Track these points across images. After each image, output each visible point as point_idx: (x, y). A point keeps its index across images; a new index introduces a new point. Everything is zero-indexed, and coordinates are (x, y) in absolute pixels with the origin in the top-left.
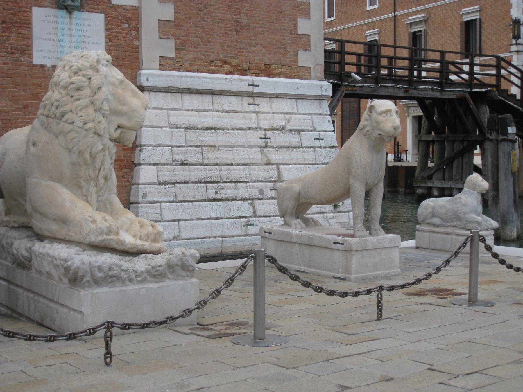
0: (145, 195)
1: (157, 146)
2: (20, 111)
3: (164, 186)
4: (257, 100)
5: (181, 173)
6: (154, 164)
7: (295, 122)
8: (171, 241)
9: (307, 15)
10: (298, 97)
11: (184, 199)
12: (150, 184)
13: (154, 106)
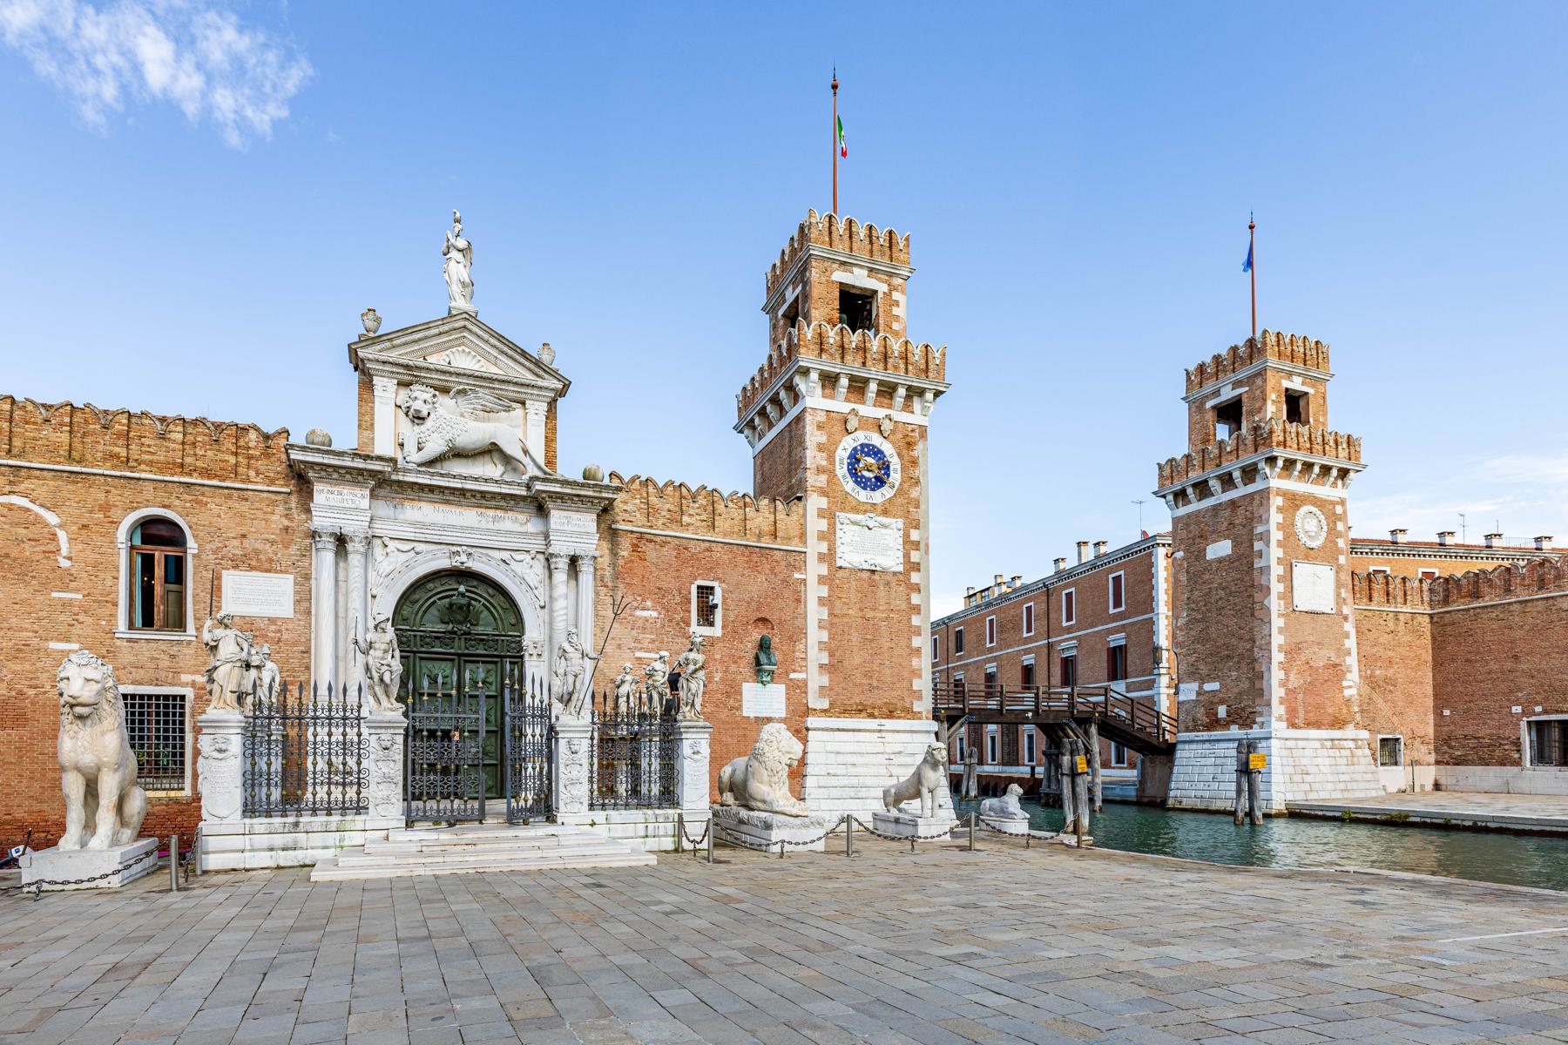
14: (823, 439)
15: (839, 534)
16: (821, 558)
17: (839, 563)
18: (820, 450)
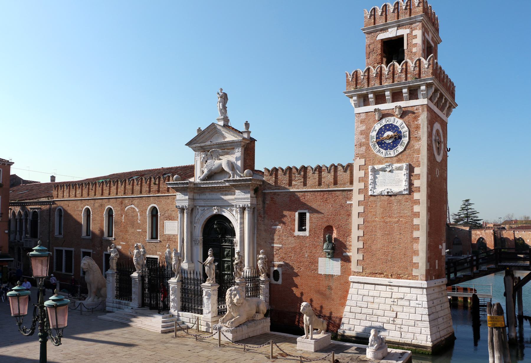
0: (345, 315)
4: (393, 288)
5: (358, 310)
7: (408, 297)
9: (418, 255)
10: (411, 287)
14: (364, 128)
15: (370, 177)
16: (360, 191)
17: (370, 193)
18: (361, 134)
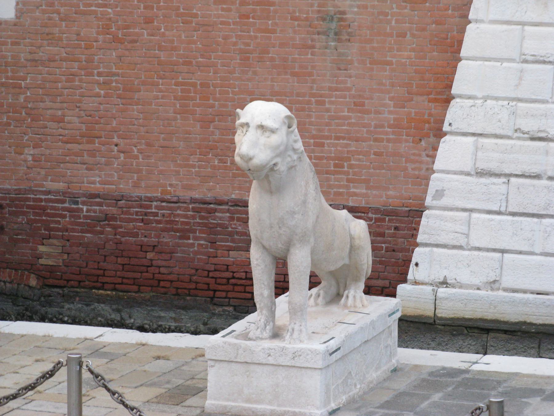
0: (439, 194)
1: (485, 98)
2: (234, 23)
3: (483, 180)
5: (528, 157)
6: (474, 135)
8: (478, 289)
11: (521, 210)
12: (455, 173)
13: (492, 17)
